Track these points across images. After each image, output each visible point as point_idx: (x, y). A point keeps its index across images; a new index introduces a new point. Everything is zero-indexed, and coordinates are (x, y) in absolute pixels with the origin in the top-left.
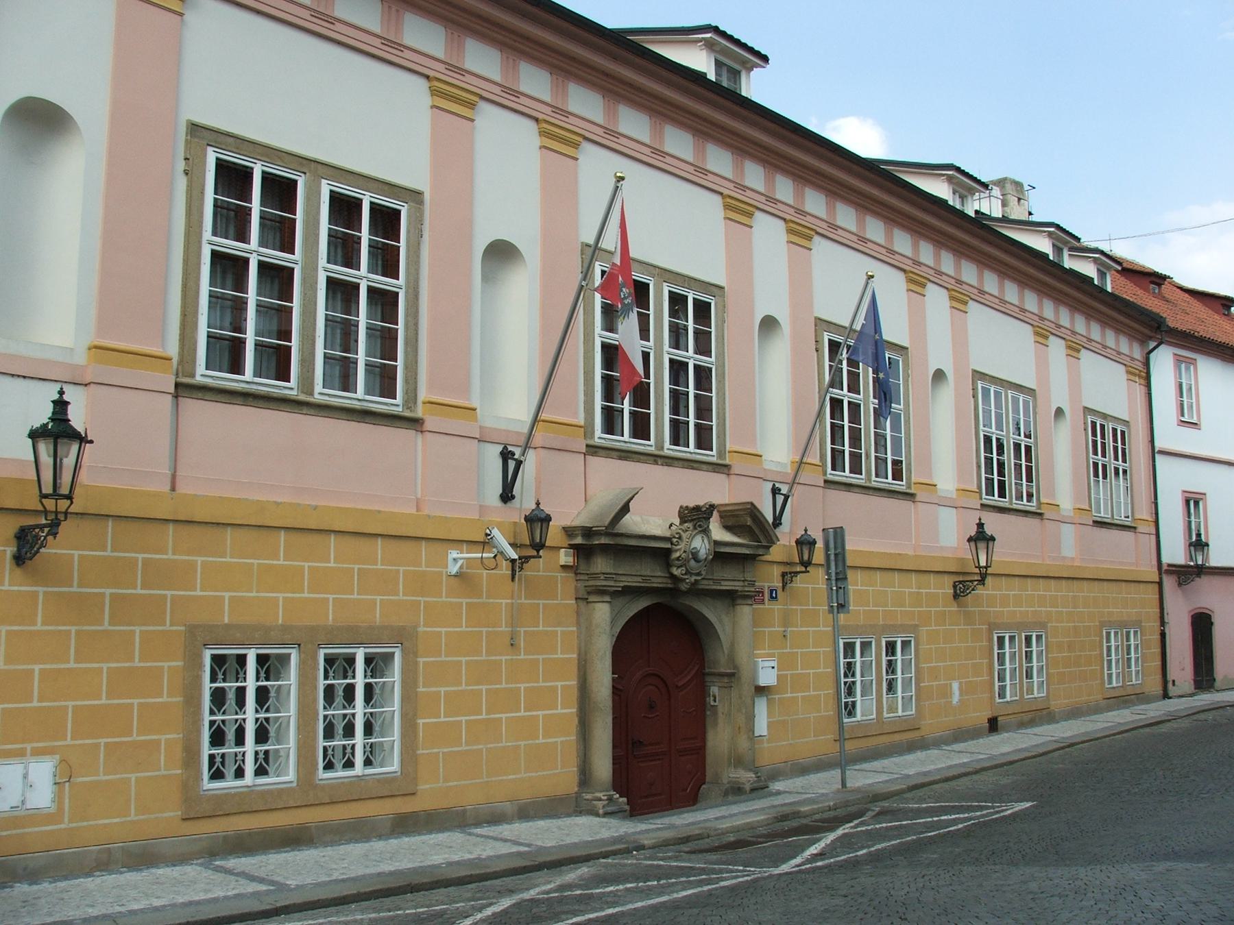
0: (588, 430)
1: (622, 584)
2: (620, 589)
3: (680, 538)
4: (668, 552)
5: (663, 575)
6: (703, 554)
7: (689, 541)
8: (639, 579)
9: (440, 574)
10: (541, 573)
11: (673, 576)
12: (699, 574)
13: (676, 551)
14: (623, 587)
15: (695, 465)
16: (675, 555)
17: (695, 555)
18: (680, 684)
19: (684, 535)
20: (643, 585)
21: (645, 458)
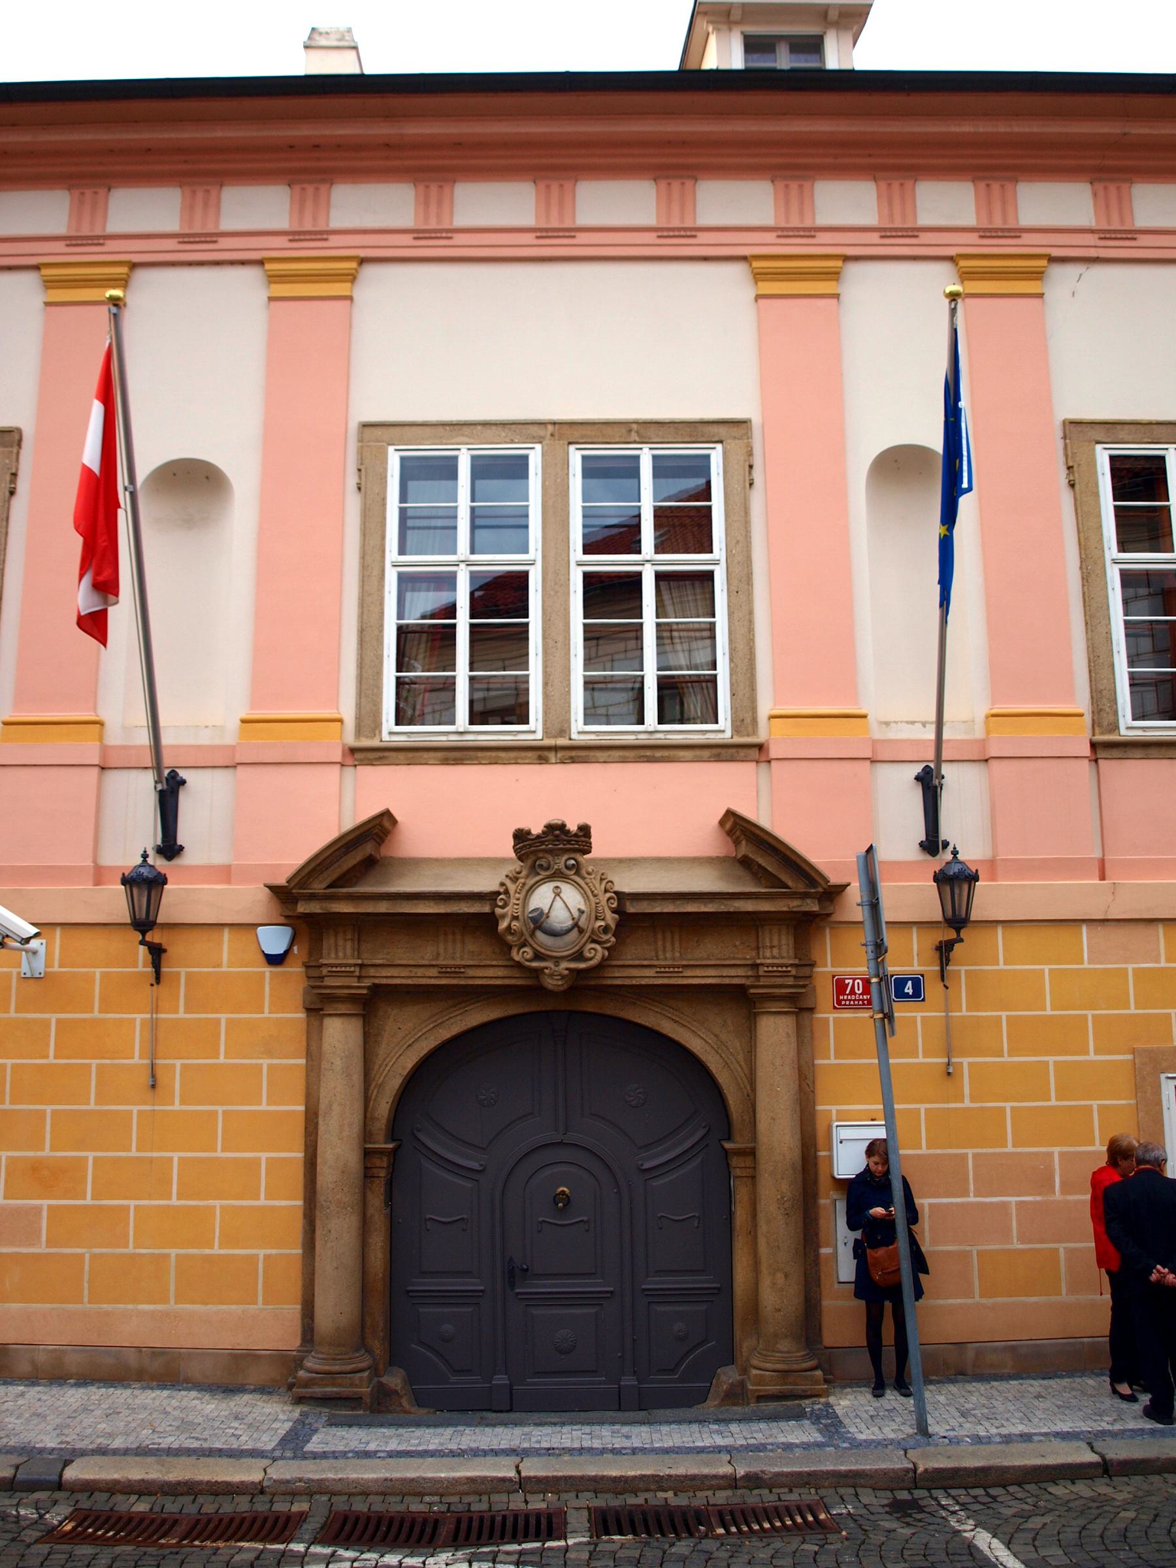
0: (368, 718)
1: (367, 983)
2: (365, 991)
3: (507, 892)
4: (490, 920)
5: (500, 963)
6: (560, 917)
7: (521, 896)
8: (434, 972)
9: (9, 975)
10: (224, 969)
11: (519, 965)
12: (579, 956)
13: (503, 916)
14: (368, 988)
15: (658, 754)
16: (503, 925)
17: (538, 921)
18: (647, 1165)
19: (512, 887)
20: (443, 982)
21: (512, 754)
